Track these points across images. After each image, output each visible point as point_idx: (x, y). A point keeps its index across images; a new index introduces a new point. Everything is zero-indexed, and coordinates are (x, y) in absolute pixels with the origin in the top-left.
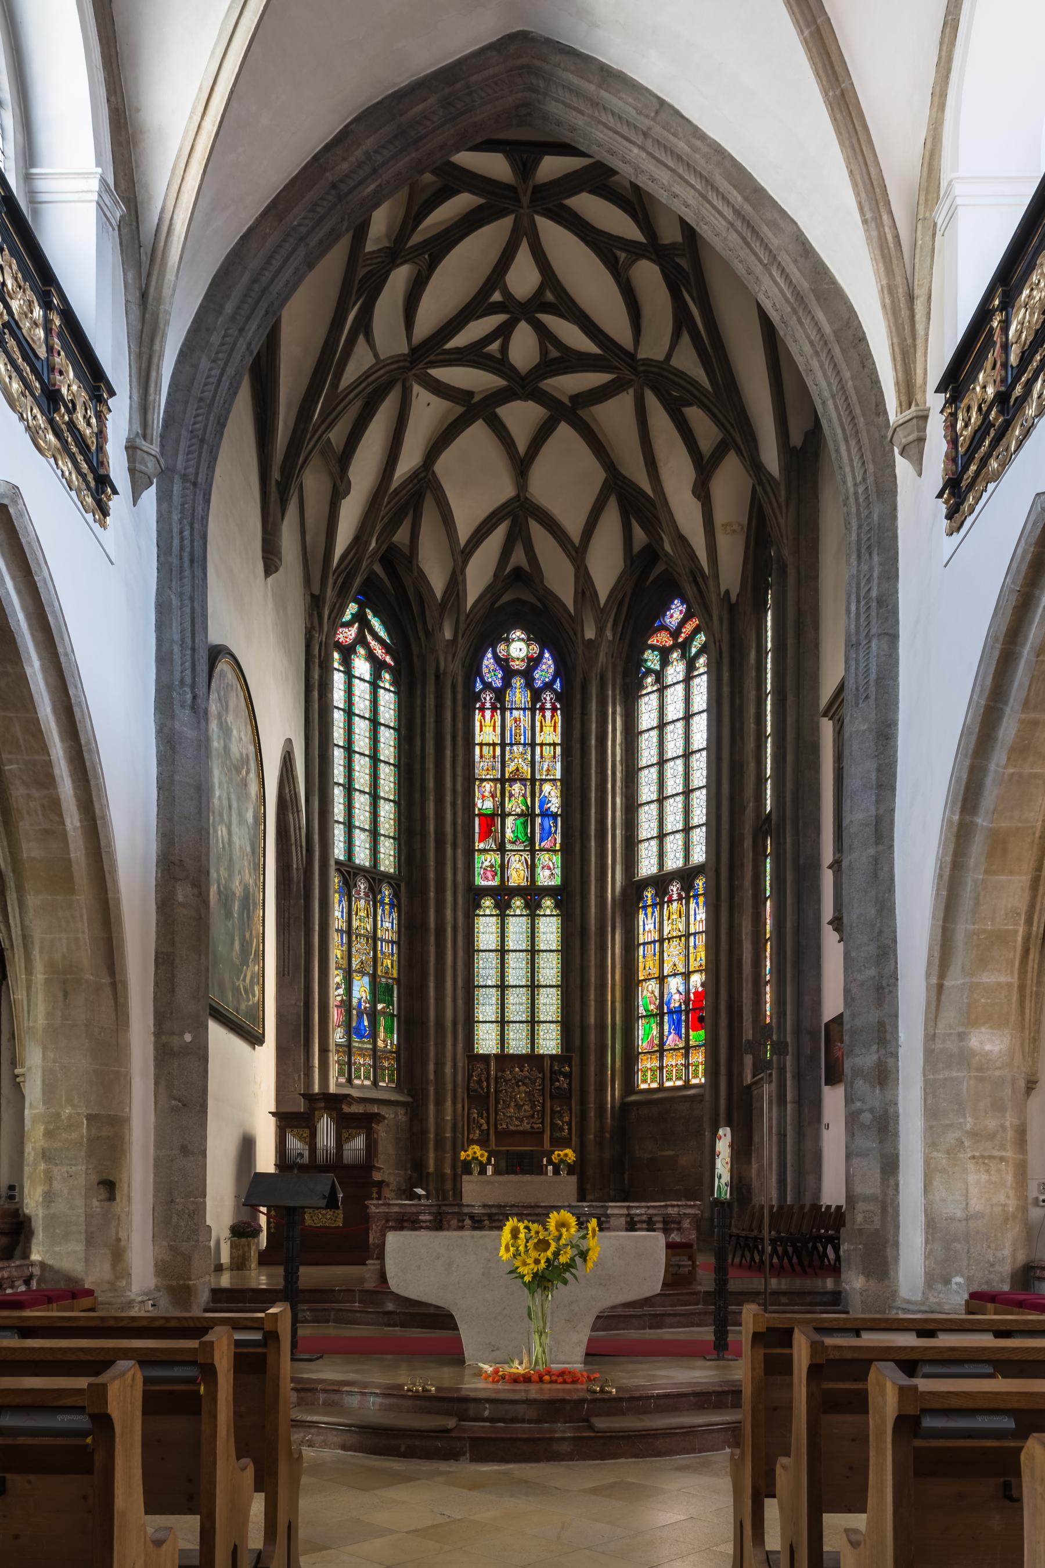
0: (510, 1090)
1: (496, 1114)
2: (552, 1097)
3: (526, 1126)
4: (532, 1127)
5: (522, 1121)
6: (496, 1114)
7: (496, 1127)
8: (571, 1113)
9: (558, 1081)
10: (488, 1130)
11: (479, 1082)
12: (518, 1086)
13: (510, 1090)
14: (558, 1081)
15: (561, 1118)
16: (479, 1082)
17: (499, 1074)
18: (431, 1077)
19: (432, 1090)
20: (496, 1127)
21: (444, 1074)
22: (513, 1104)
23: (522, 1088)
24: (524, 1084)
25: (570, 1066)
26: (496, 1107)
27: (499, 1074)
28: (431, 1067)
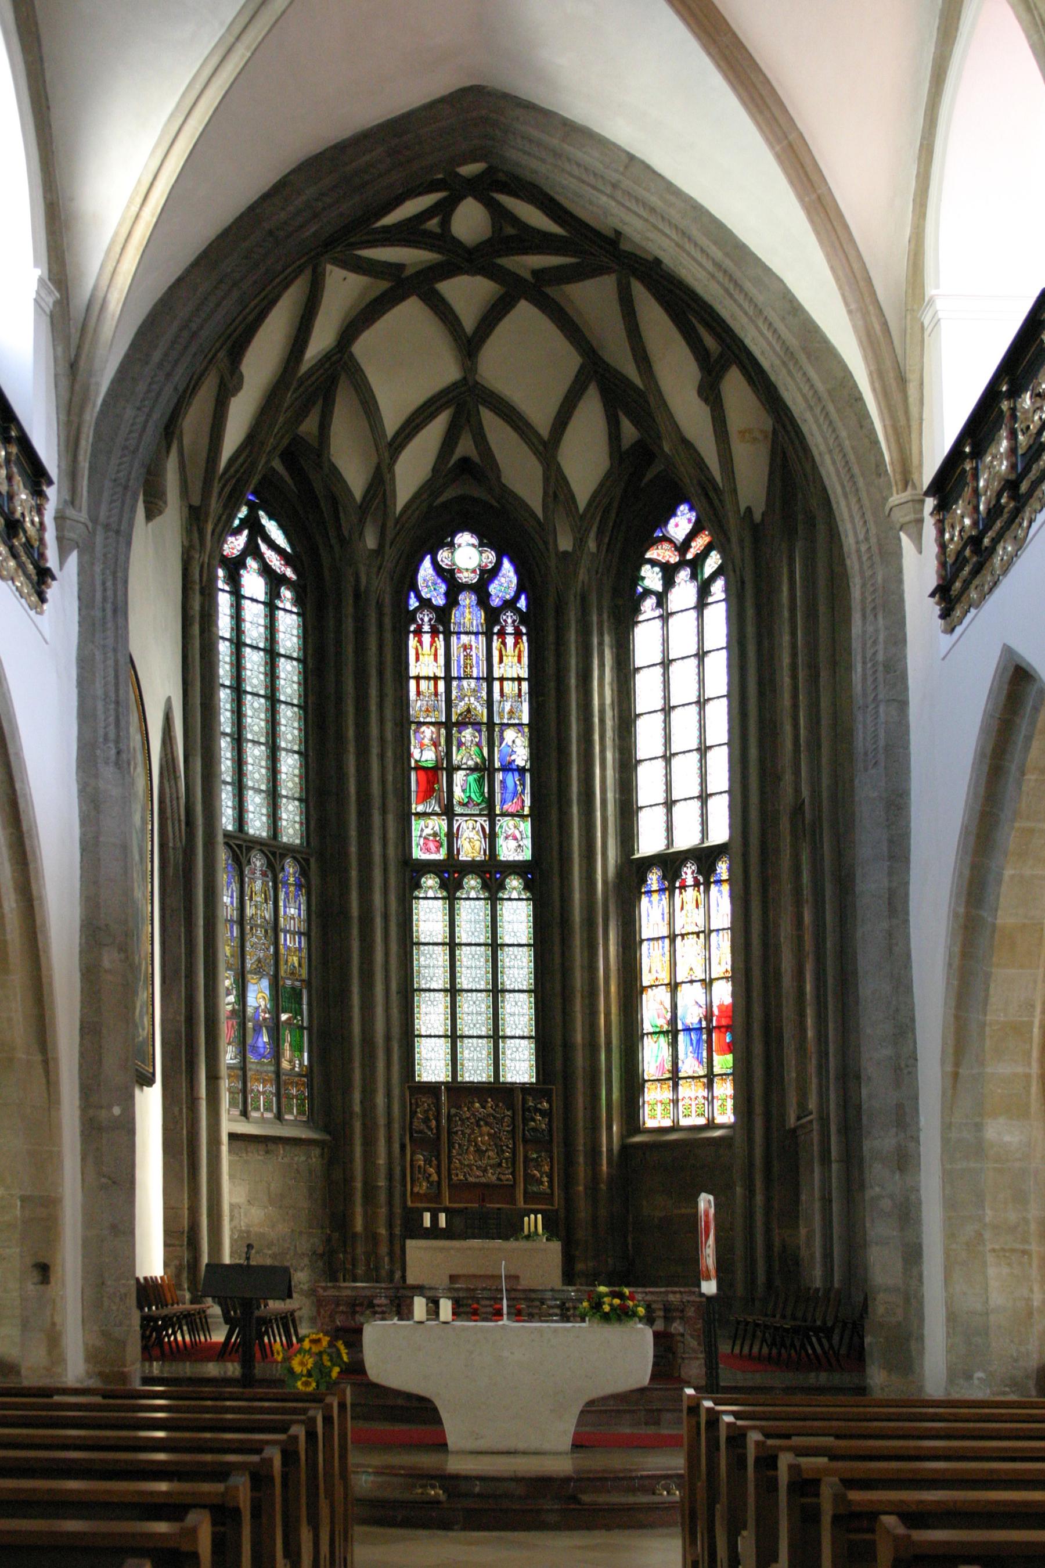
0: (468, 1131)
1: (450, 1162)
2: (525, 1141)
3: (491, 1177)
4: (499, 1179)
5: (485, 1171)
6: (450, 1162)
7: (450, 1179)
8: (552, 1161)
9: (534, 1120)
10: (439, 1183)
11: (426, 1121)
14: (534, 1120)
15: (538, 1167)
16: (426, 1121)
17: (453, 1111)
18: (357, 1108)
19: (358, 1126)
20: (450, 1179)
21: (374, 1106)
23: (485, 1129)
24: (487, 1124)
25: (549, 1102)
26: (450, 1151)
28: (357, 1096)
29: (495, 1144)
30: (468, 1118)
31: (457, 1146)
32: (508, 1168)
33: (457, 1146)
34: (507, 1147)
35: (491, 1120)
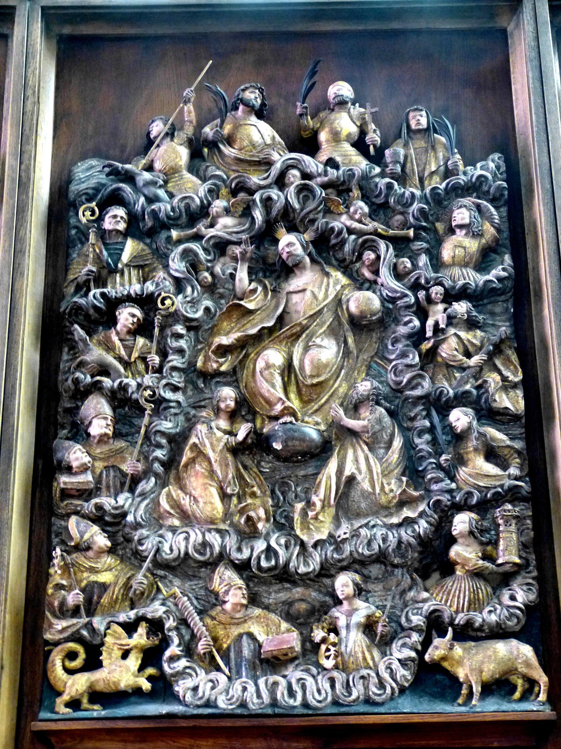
12: (275, 271)
13: (190, 304)
24: (325, 249)
27: (89, 174)
31: (99, 416)
33: (99, 416)
34: (488, 414)
35: (352, 219)
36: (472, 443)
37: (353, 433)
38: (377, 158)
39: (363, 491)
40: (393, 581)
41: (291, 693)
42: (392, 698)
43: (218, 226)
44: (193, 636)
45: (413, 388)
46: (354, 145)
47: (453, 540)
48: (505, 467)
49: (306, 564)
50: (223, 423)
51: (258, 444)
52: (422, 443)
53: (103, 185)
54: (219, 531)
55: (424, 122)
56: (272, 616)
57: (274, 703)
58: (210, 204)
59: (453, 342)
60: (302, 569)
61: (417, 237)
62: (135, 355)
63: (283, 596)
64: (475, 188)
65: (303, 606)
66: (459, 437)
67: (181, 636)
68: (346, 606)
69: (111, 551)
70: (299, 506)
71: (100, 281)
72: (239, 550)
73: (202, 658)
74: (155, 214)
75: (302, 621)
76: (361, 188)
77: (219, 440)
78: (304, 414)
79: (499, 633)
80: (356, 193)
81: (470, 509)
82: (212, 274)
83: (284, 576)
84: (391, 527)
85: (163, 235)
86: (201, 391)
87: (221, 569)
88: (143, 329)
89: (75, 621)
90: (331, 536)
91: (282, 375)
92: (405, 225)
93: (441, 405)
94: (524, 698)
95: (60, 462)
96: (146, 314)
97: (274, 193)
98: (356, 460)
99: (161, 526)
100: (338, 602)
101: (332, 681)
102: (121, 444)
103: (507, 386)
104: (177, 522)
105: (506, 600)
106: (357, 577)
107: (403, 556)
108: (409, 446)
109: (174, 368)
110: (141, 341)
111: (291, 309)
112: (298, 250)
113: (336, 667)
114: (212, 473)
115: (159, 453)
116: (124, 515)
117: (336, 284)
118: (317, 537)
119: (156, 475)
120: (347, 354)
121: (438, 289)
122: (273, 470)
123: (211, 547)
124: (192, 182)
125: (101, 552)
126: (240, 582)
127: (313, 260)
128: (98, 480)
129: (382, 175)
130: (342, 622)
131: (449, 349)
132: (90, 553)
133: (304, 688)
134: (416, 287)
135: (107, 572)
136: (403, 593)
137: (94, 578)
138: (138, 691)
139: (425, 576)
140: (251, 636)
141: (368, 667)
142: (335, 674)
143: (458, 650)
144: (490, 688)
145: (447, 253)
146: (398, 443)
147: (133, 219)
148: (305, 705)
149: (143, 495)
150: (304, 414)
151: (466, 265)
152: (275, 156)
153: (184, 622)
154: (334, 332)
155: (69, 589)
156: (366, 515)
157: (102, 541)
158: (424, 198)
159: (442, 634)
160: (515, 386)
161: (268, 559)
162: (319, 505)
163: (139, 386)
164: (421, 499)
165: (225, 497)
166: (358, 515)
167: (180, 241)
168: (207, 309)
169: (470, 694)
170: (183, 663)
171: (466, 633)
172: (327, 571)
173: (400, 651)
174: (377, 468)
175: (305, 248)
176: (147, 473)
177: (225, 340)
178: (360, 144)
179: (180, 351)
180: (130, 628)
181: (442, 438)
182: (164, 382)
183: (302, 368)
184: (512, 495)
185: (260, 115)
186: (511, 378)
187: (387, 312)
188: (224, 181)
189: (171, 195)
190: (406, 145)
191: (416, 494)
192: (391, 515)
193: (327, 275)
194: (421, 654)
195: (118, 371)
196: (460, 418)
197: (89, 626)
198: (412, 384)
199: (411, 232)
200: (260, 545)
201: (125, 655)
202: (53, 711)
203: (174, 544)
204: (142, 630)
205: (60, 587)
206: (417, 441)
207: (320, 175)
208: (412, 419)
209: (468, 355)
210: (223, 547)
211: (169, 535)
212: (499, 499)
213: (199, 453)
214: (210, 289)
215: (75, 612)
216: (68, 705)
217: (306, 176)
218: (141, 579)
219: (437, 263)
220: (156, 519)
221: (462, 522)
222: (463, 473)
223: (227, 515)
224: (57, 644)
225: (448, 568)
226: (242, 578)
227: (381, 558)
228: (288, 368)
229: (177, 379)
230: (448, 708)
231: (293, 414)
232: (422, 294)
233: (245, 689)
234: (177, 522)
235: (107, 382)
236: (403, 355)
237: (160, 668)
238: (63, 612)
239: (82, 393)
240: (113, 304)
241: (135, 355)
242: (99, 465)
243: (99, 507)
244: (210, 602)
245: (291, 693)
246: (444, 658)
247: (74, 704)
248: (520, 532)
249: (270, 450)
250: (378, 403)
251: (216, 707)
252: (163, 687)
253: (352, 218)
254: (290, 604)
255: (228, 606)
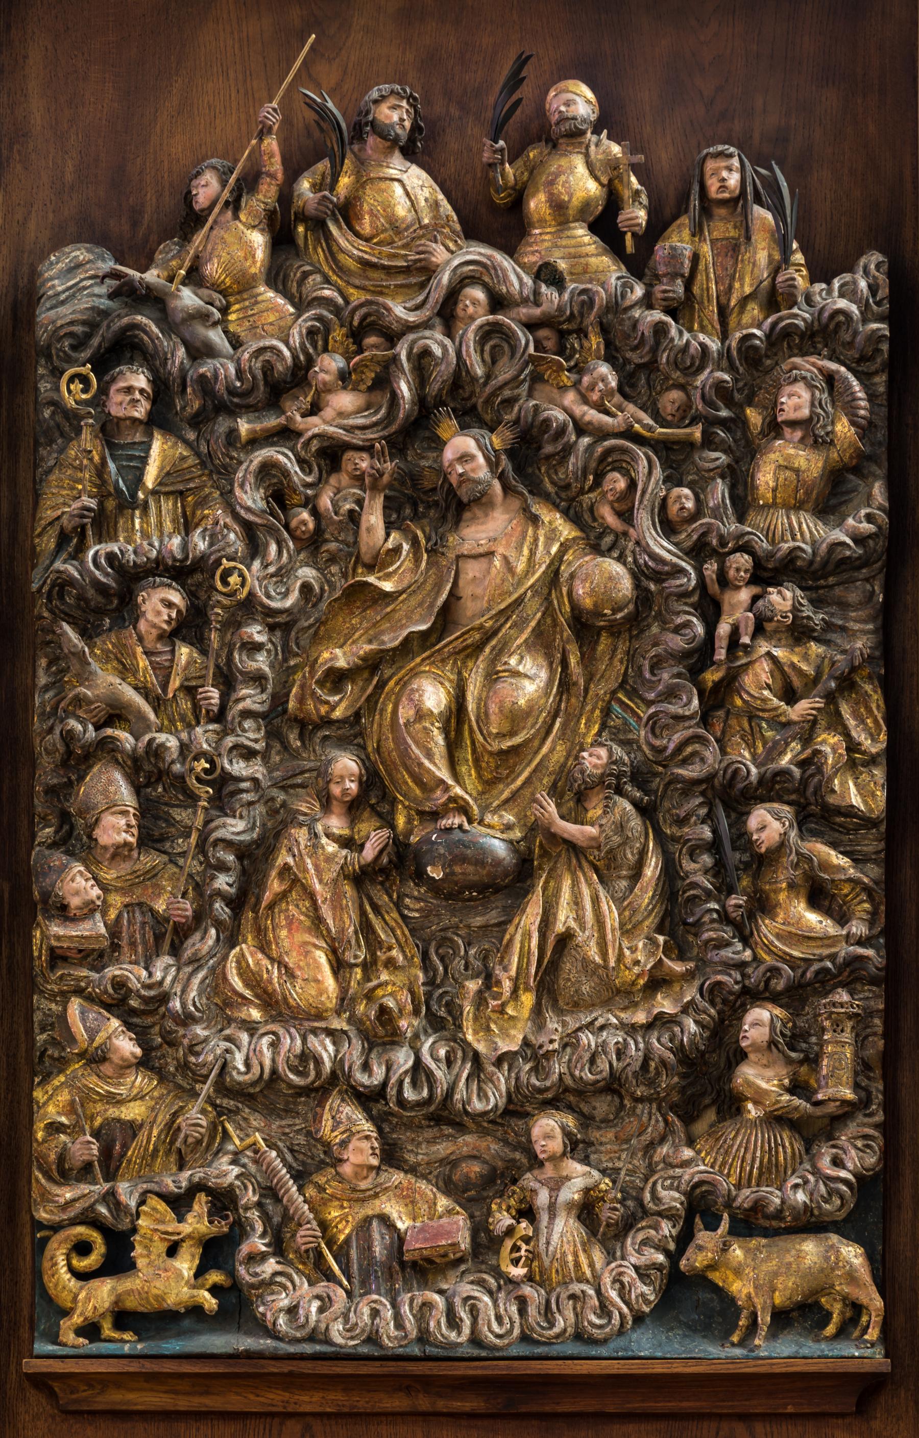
0: (276, 579)
4: (687, 1296)
5: (496, 1181)
13: (276, 579)
22: (320, 848)
23: (509, 547)
24: (530, 460)
29: (646, 783)
30: (283, 384)
32: (813, 1130)
34: (818, 814)
35: (583, 401)
36: (783, 875)
37: (572, 847)
38: (637, 265)
39: (586, 962)
40: (632, 1125)
41: (453, 1322)
42: (621, 1332)
43: (328, 413)
44: (287, 1217)
45: (685, 762)
46: (594, 228)
47: (741, 1056)
48: (842, 919)
49: (482, 1095)
50: (336, 824)
51: (402, 861)
52: (697, 871)
53: (104, 314)
54: (330, 1032)
55: (733, 180)
56: (423, 1185)
57: (424, 1337)
58: (310, 362)
59: (763, 671)
60: (478, 1105)
61: (709, 442)
62: (175, 683)
63: (443, 1149)
64: (825, 334)
65: (475, 1168)
66: (762, 862)
67: (266, 1218)
68: (549, 1171)
69: (144, 1063)
70: (473, 986)
71: (102, 523)
72: (366, 1067)
73: (303, 1257)
74: (205, 384)
75: (474, 1195)
76: (605, 330)
77: (329, 859)
78: (484, 809)
79: (809, 1224)
80: (595, 341)
81: (775, 999)
82: (315, 513)
83: (443, 1115)
84: (631, 1029)
85: (222, 425)
86: (295, 755)
87: (334, 1101)
88: (189, 627)
89: (85, 1188)
90: (526, 1043)
91: (445, 731)
92: (686, 415)
93: (732, 797)
94: (842, 1333)
95: (46, 895)
96: (191, 594)
97: (436, 342)
98: (577, 902)
99: (230, 1020)
100: (536, 1163)
101: (522, 1303)
102: (150, 860)
103: (855, 757)
104: (256, 1014)
105: (825, 1164)
106: (570, 1121)
107: (651, 1083)
108: (670, 873)
109: (247, 714)
110: (184, 652)
111: (466, 590)
112: (480, 469)
113: (530, 1278)
114: (318, 921)
115: (223, 882)
116: (164, 998)
117: (550, 540)
118: (505, 1046)
119: (218, 924)
120: (565, 685)
121: (743, 560)
122: (427, 914)
123: (318, 1062)
124: (275, 309)
125: (125, 1067)
126: (367, 1126)
127: (507, 489)
128: (114, 931)
129: (648, 302)
130: (543, 1197)
131: (758, 681)
132: (106, 1069)
133: (474, 1312)
134: (699, 551)
135: (136, 1101)
136: (651, 1146)
137: (113, 1112)
138: (196, 1310)
139: (689, 1119)
140: (385, 1220)
141: (581, 1279)
142: (527, 1290)
143: (737, 1253)
144: (782, 1319)
145: (766, 477)
146: (652, 869)
147: (162, 392)
148: (475, 1340)
149: (196, 962)
150: (484, 809)
151: (798, 507)
152: (439, 254)
153: (271, 1192)
154: (542, 642)
155: (74, 1130)
156: (592, 1006)
157: (127, 1046)
158: (726, 353)
159: (712, 1227)
160: (872, 761)
161: (415, 1084)
162: (507, 985)
163: (184, 748)
164: (689, 976)
165: (339, 966)
166: (577, 1005)
167: (254, 442)
168: (306, 588)
169: (753, 1325)
170: (271, 1266)
171: (752, 1223)
172: (517, 1109)
173: (642, 1253)
174: (612, 916)
175: (493, 465)
176: (200, 917)
177: (340, 657)
178: (605, 223)
179: (258, 679)
180: (179, 1203)
181: (734, 857)
182: (230, 741)
183: (483, 717)
184: (850, 973)
185: (409, 153)
186: (867, 743)
187: (643, 598)
188: (337, 311)
189: (236, 343)
190: (697, 231)
191: (678, 967)
192: (634, 1005)
193: (535, 520)
194: (674, 1257)
195: (142, 717)
196: (768, 823)
197: (110, 1198)
198: (681, 756)
199: (697, 433)
200: (403, 1059)
201: (172, 1251)
202: (55, 1341)
203: (252, 1053)
204: (201, 1204)
205: (55, 1128)
206: (688, 865)
207: (525, 301)
208: (681, 822)
209: (790, 696)
210: (338, 1062)
211: (244, 1037)
212: (825, 981)
213: (294, 879)
214: (312, 544)
215: (85, 1172)
216: (80, 1331)
217: (498, 302)
218: (196, 1116)
219: (743, 501)
220: (222, 1006)
221: (760, 1021)
222: (767, 928)
223: (345, 1002)
224: (56, 1228)
225: (731, 1105)
226: (371, 1118)
227: (613, 1085)
228: (455, 718)
229: (252, 735)
230: (714, 1350)
231: (464, 810)
232: (711, 568)
233: (375, 1313)
234: (256, 1014)
235: (125, 738)
236: (671, 694)
237: (232, 1274)
238: (65, 1172)
239: (78, 760)
240: (131, 578)
241: (175, 683)
242: (117, 900)
243: (120, 984)
244: (314, 1161)
245: (453, 1322)
246: (713, 1266)
247: (90, 1330)
248: (860, 1041)
249: (420, 876)
250: (619, 791)
251: (328, 1342)
252: (237, 1306)
253: (585, 400)
254: (452, 1163)
255: (347, 1169)
